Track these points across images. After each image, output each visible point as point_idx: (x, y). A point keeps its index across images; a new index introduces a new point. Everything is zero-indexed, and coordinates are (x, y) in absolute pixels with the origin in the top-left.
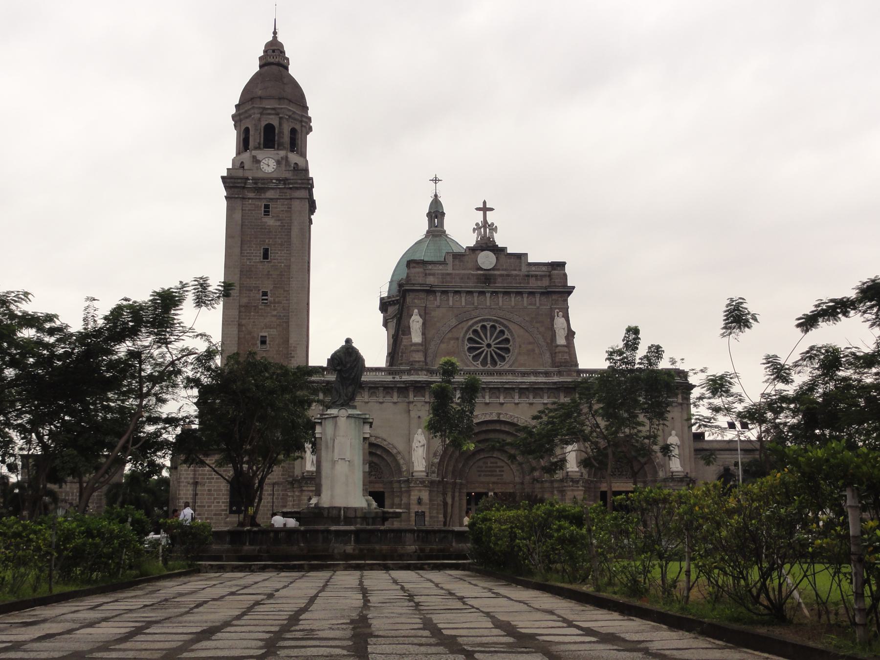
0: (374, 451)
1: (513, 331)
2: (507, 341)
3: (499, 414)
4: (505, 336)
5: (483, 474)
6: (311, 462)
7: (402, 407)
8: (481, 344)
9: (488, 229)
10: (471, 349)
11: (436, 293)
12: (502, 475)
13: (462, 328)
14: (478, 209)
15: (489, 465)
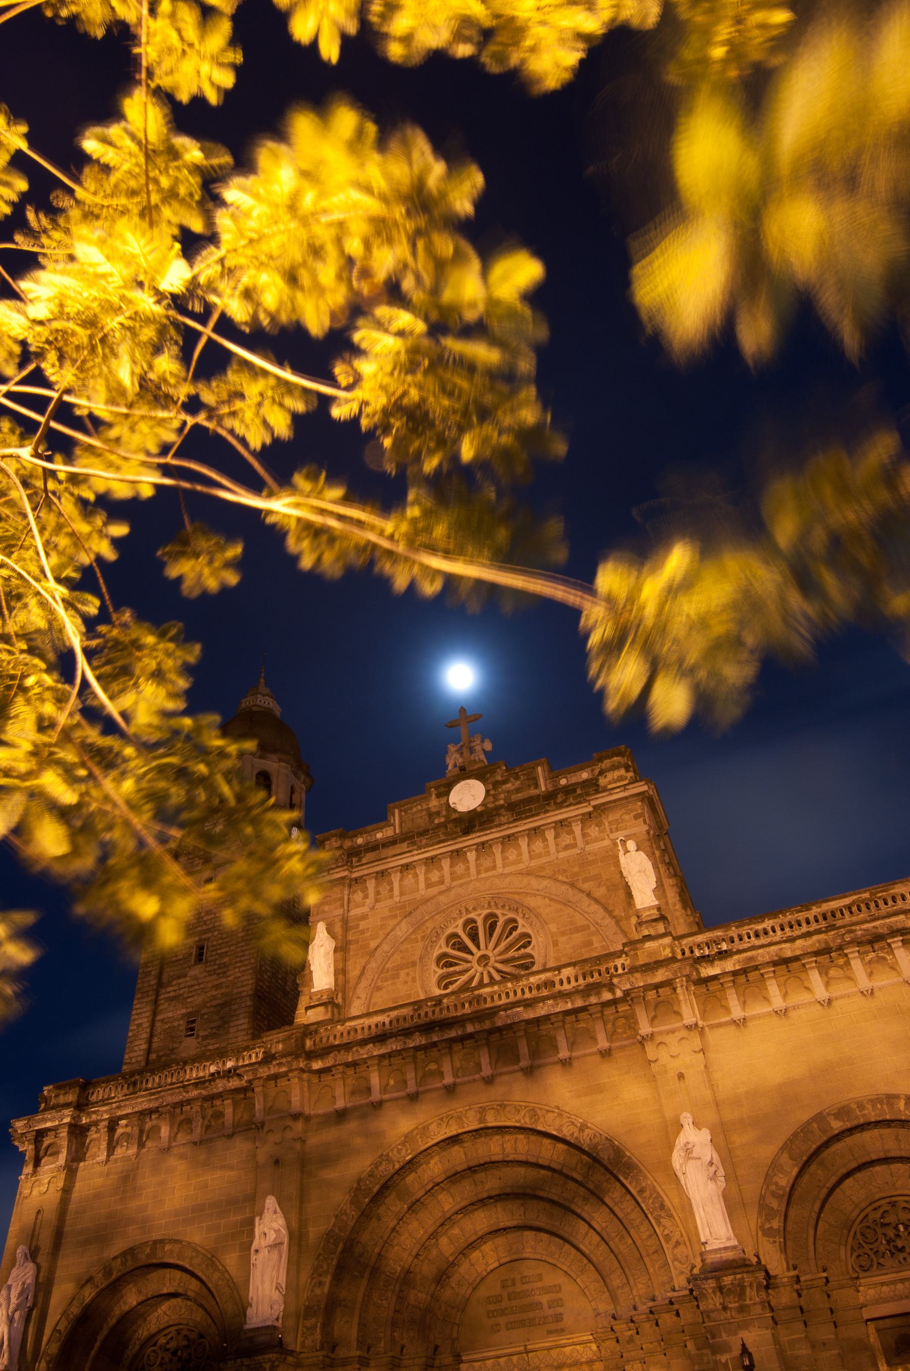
5: (502, 1320)
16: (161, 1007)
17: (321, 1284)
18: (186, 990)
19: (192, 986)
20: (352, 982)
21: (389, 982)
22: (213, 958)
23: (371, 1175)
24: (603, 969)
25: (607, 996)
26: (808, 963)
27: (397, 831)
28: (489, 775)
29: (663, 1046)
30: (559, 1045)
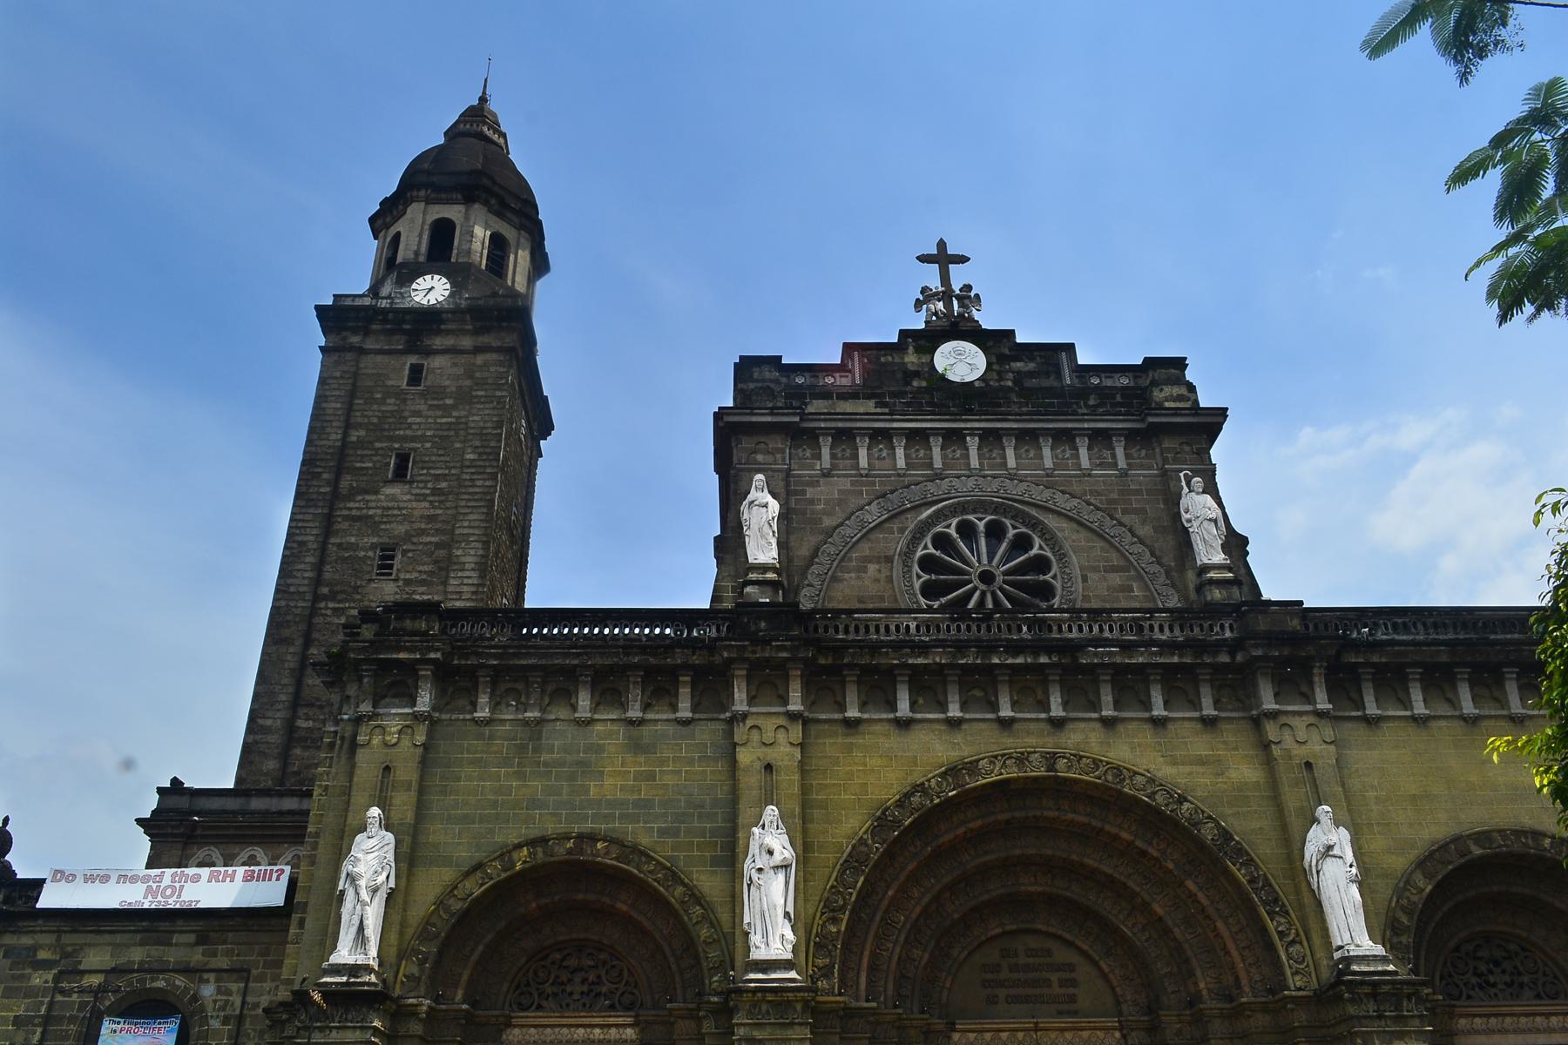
0: (606, 900)
1: (1059, 534)
2: (1041, 564)
3: (1051, 759)
4: (1035, 551)
5: (1002, 993)
6: (354, 930)
7: (708, 733)
8: (963, 572)
9: (955, 303)
10: (929, 590)
11: (817, 438)
12: (1072, 999)
13: (902, 531)
14: (924, 259)
15: (1022, 960)
16: (337, 526)
17: (835, 921)
18: (379, 512)
19: (389, 508)
20: (797, 563)
21: (853, 575)
22: (422, 478)
23: (900, 804)
24: (1206, 625)
25: (1224, 658)
26: (1461, 673)
27: (857, 382)
28: (991, 344)
29: (1287, 728)
30: (1153, 700)
